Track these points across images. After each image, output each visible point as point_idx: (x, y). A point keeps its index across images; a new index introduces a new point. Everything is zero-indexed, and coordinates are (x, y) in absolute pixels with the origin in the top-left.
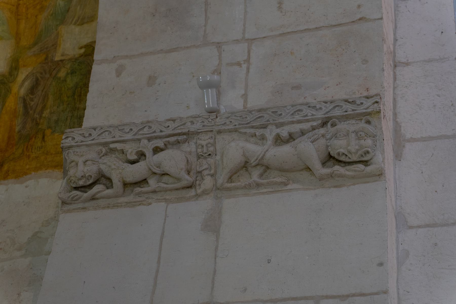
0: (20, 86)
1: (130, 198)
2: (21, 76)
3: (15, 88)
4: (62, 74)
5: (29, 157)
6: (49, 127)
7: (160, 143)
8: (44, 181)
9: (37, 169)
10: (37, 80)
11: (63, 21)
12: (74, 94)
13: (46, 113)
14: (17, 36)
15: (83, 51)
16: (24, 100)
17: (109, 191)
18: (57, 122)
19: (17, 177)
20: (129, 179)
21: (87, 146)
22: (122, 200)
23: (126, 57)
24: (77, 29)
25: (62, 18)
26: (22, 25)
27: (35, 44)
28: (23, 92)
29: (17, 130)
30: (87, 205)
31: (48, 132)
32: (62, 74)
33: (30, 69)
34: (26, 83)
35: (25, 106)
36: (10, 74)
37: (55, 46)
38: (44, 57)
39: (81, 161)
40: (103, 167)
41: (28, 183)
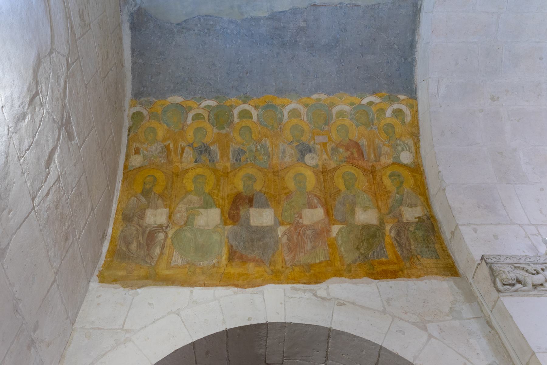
0: (389, 231)
1: (535, 292)
2: (388, 227)
3: (387, 233)
4: (412, 229)
5: (416, 268)
6: (418, 254)
7: (542, 266)
8: (434, 281)
9: (427, 274)
10: (398, 230)
11: (401, 204)
12: (424, 240)
13: (413, 247)
14: (378, 208)
15: (417, 220)
16: (396, 240)
17: (525, 288)
18: (421, 252)
19: (417, 277)
20: (535, 283)
21: (501, 264)
22: (531, 293)
23: (474, 224)
24: (410, 209)
25: (401, 202)
26: (380, 203)
27: (390, 213)
28: (393, 234)
29: (399, 253)
30: (512, 294)
31: (419, 257)
32: (412, 229)
33: (391, 225)
34: (393, 231)
35: (398, 242)
36: (381, 225)
37: (401, 215)
38: (397, 220)
39: (506, 270)
40: (518, 275)
41: (426, 281)
